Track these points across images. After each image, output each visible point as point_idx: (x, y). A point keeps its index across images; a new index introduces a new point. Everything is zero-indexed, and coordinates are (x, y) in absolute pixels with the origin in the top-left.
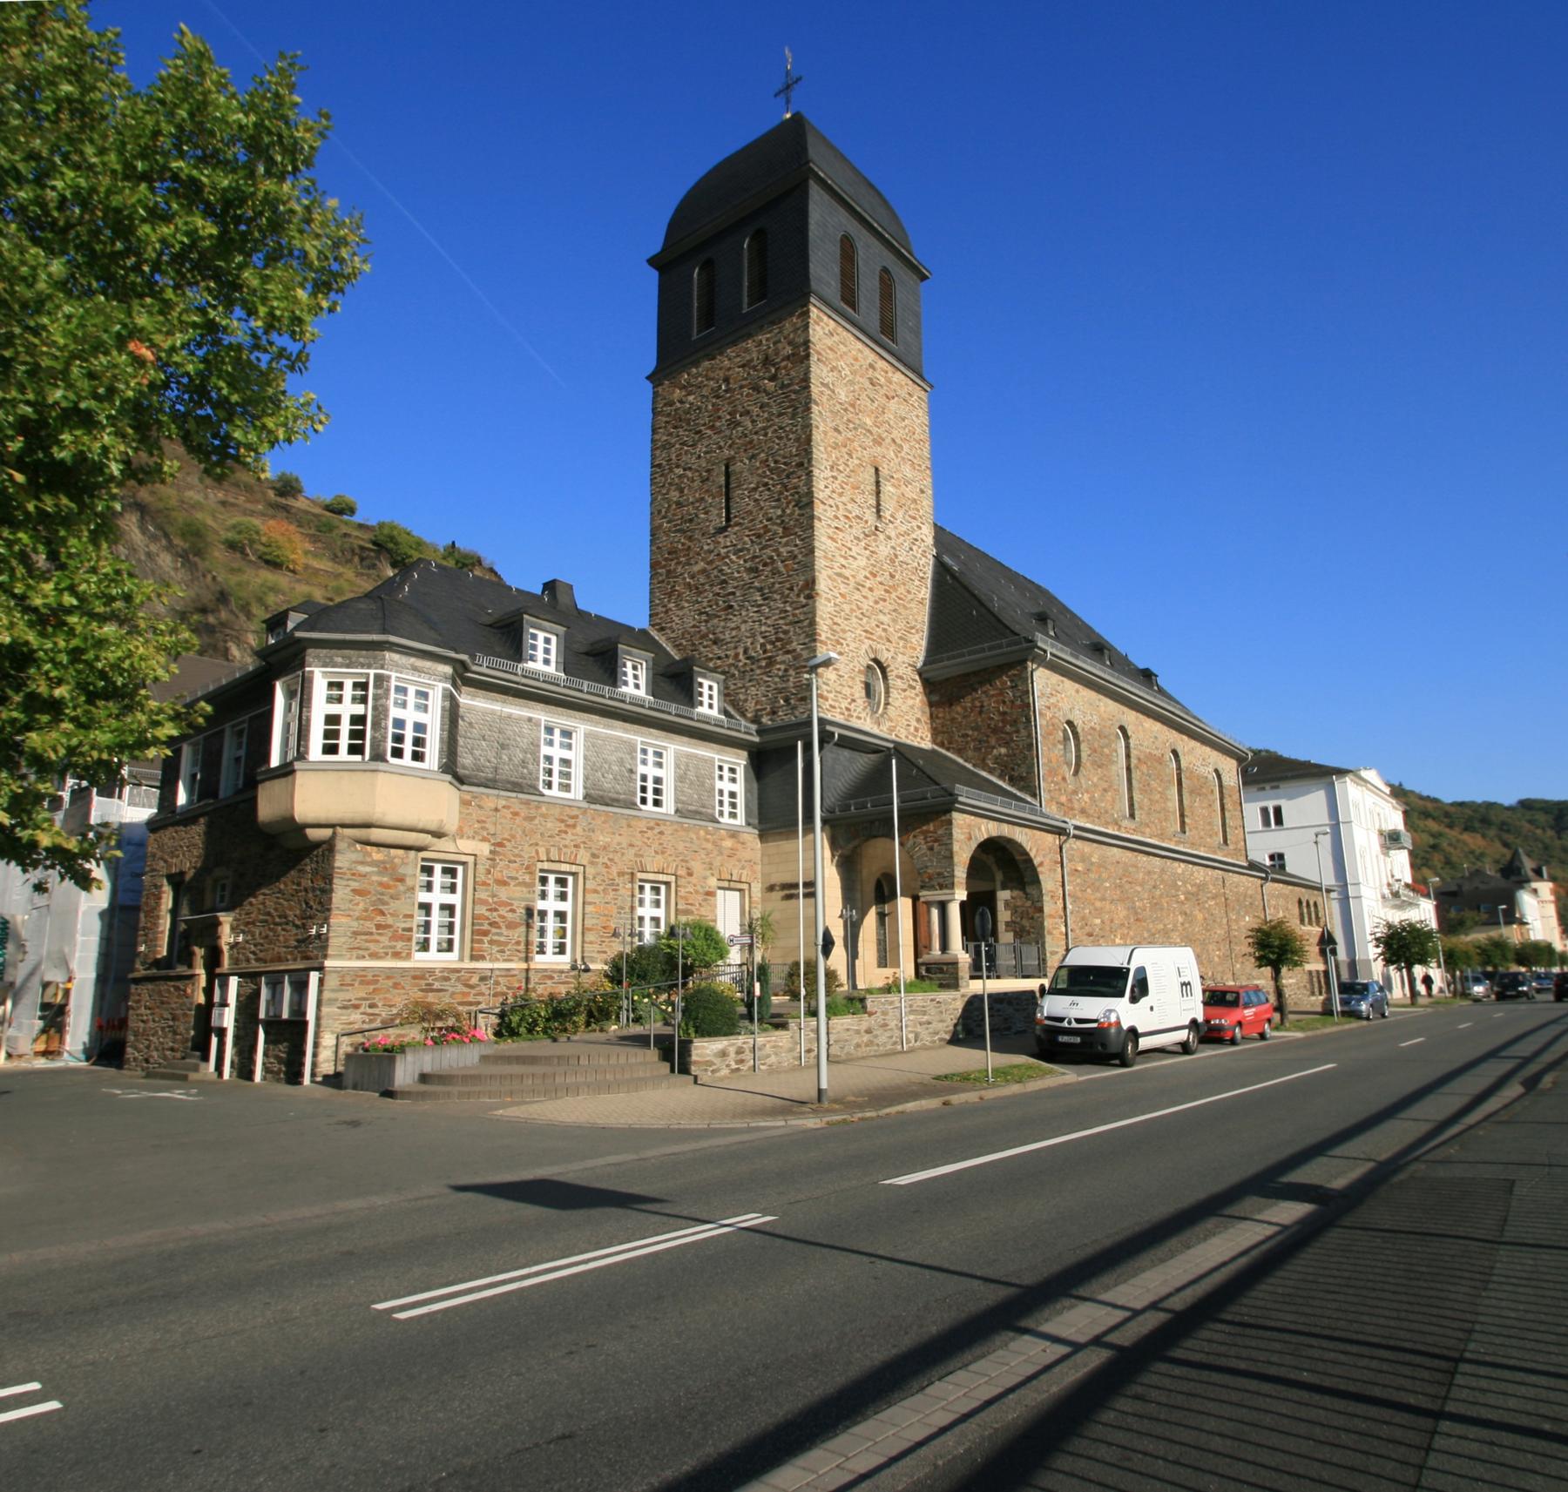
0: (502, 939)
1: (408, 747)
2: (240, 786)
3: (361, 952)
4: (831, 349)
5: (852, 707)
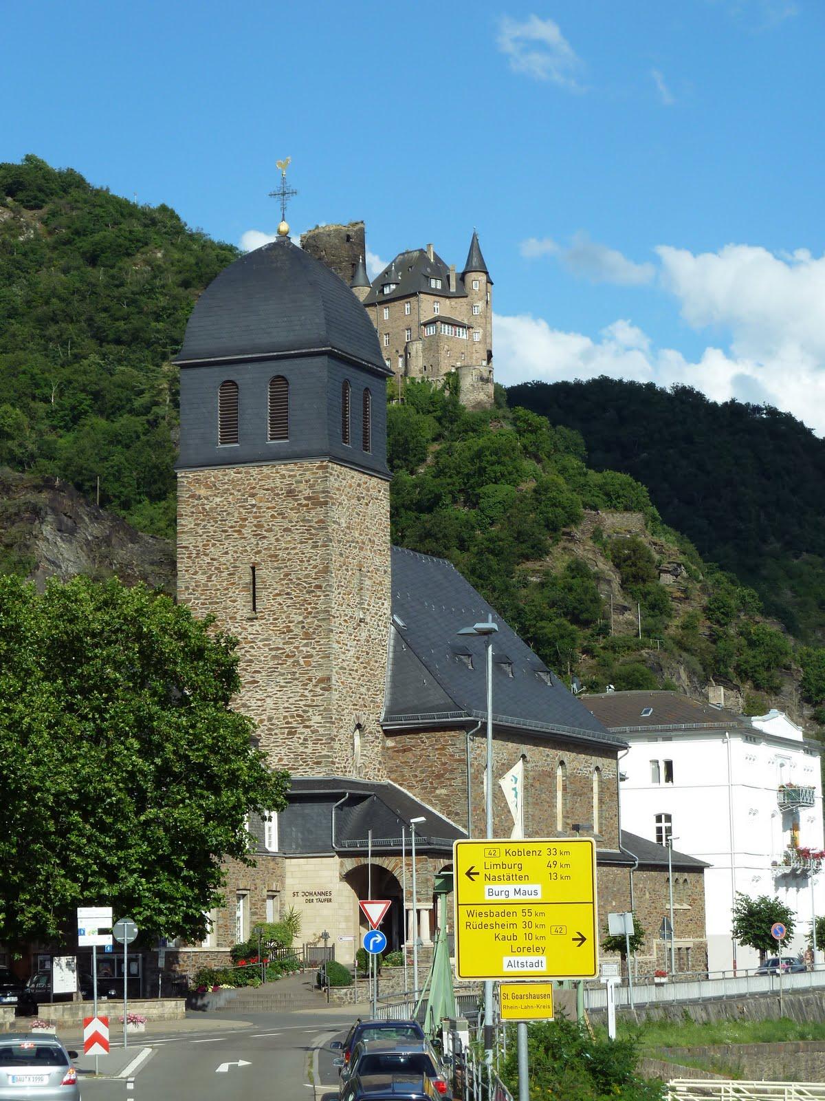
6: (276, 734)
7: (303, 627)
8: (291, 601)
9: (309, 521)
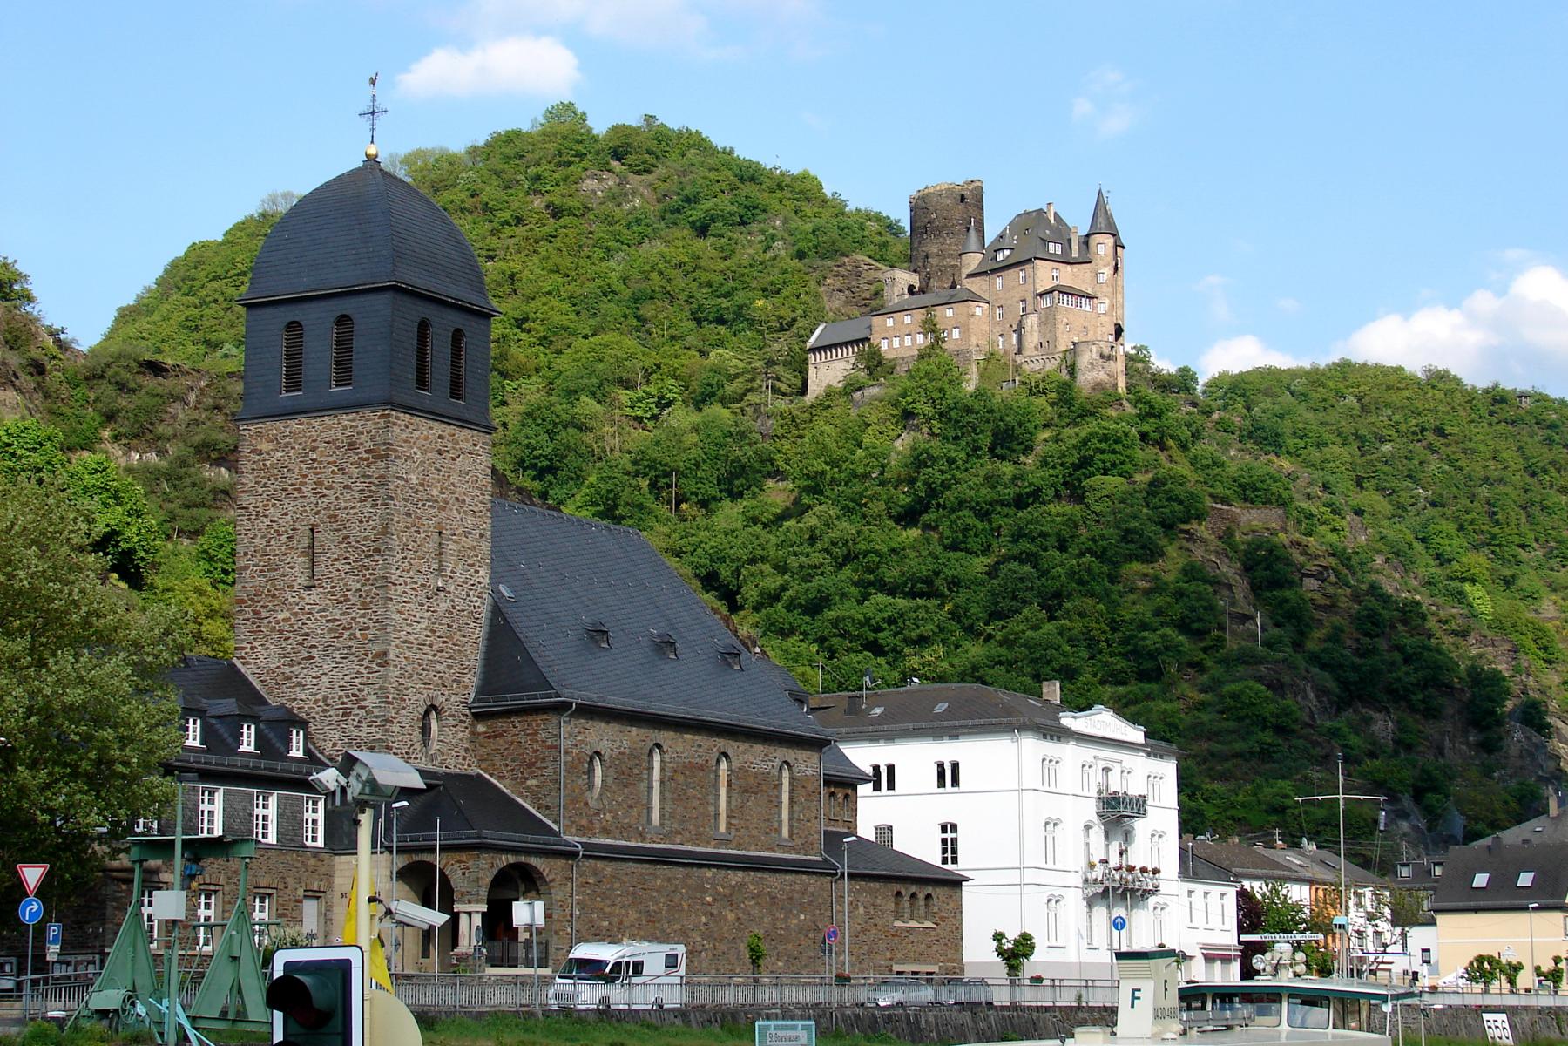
6: (331, 716)
7: (361, 596)
8: (349, 567)
9: (369, 477)
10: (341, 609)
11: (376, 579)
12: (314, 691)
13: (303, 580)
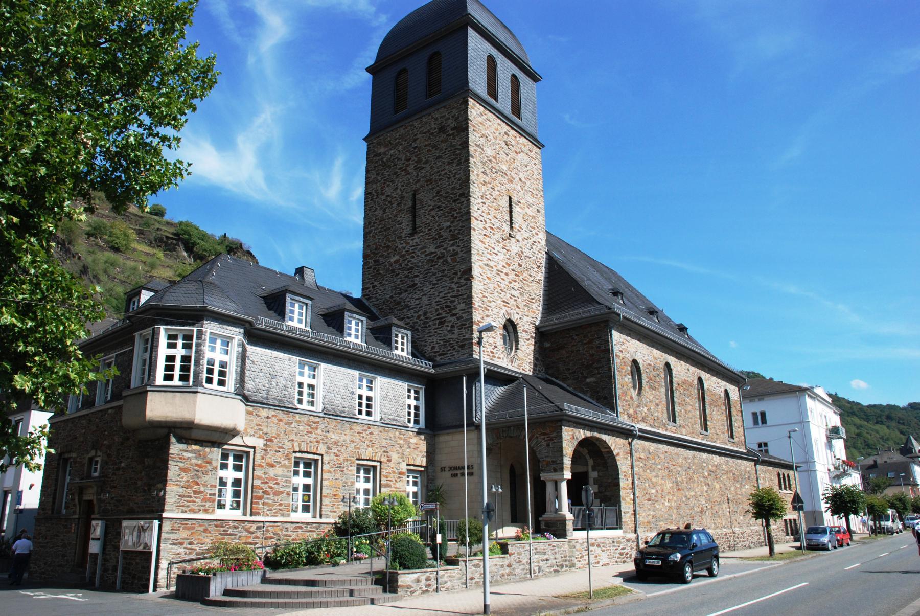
0: (270, 502)
1: (216, 377)
2: (109, 398)
3: (184, 508)
4: (481, 124)
5: (495, 351)
6: (430, 326)
7: (450, 231)
10: (436, 244)
11: (461, 216)
12: (417, 309)
13: (408, 230)
